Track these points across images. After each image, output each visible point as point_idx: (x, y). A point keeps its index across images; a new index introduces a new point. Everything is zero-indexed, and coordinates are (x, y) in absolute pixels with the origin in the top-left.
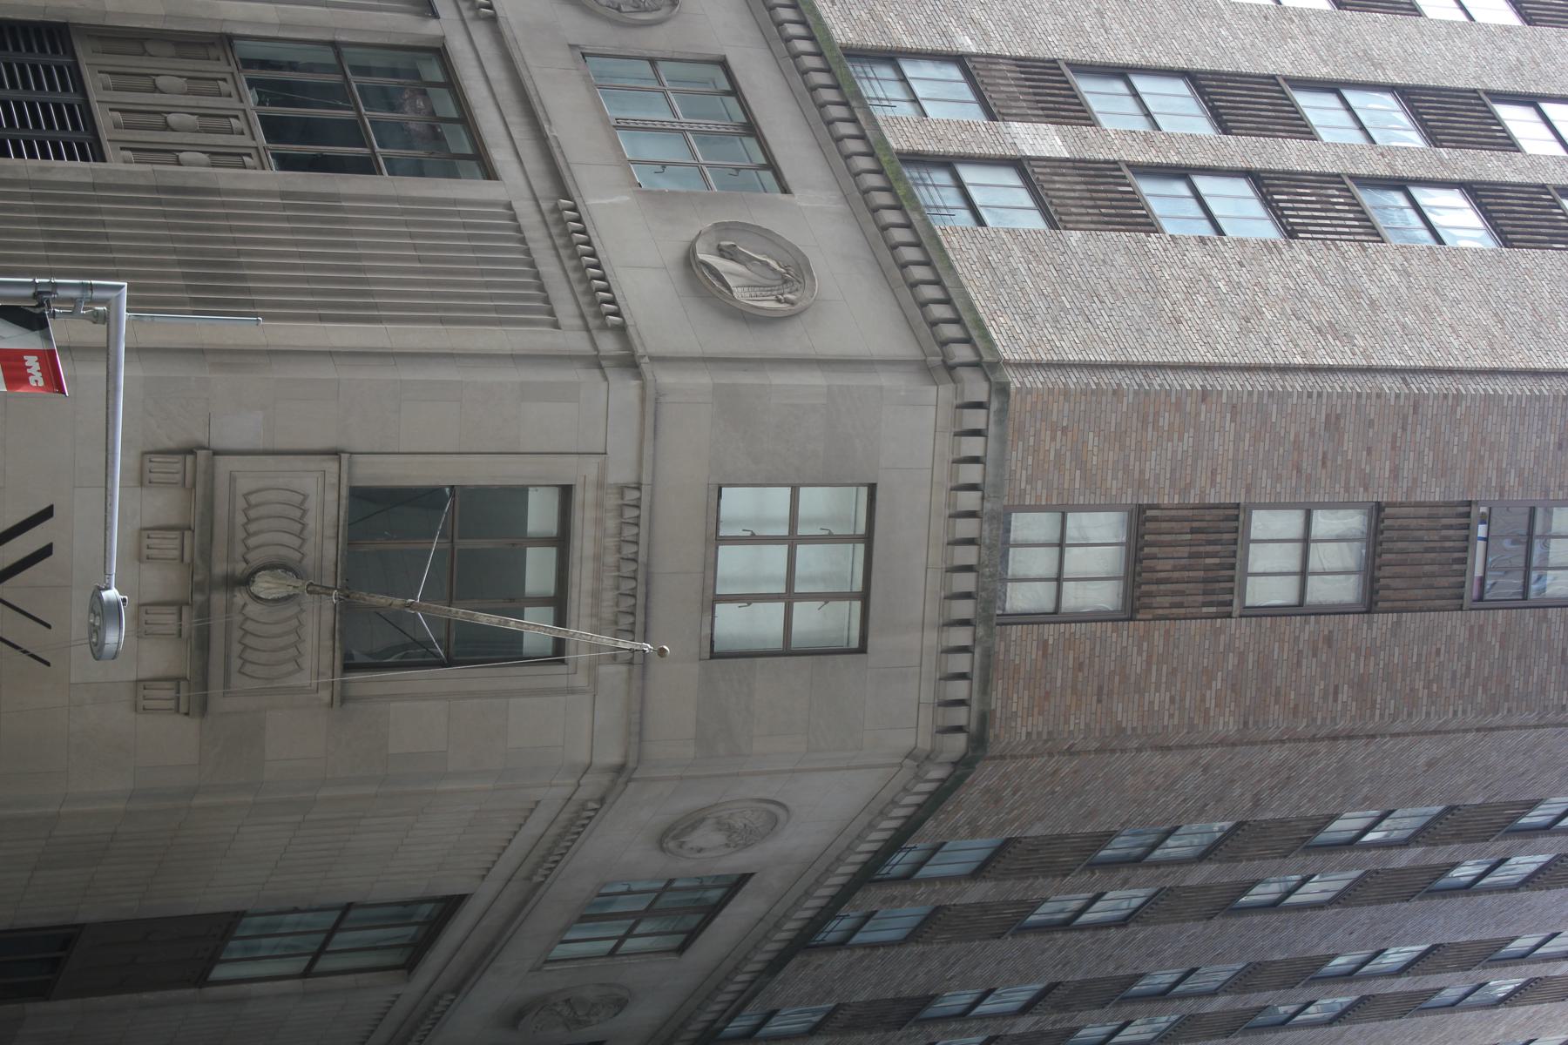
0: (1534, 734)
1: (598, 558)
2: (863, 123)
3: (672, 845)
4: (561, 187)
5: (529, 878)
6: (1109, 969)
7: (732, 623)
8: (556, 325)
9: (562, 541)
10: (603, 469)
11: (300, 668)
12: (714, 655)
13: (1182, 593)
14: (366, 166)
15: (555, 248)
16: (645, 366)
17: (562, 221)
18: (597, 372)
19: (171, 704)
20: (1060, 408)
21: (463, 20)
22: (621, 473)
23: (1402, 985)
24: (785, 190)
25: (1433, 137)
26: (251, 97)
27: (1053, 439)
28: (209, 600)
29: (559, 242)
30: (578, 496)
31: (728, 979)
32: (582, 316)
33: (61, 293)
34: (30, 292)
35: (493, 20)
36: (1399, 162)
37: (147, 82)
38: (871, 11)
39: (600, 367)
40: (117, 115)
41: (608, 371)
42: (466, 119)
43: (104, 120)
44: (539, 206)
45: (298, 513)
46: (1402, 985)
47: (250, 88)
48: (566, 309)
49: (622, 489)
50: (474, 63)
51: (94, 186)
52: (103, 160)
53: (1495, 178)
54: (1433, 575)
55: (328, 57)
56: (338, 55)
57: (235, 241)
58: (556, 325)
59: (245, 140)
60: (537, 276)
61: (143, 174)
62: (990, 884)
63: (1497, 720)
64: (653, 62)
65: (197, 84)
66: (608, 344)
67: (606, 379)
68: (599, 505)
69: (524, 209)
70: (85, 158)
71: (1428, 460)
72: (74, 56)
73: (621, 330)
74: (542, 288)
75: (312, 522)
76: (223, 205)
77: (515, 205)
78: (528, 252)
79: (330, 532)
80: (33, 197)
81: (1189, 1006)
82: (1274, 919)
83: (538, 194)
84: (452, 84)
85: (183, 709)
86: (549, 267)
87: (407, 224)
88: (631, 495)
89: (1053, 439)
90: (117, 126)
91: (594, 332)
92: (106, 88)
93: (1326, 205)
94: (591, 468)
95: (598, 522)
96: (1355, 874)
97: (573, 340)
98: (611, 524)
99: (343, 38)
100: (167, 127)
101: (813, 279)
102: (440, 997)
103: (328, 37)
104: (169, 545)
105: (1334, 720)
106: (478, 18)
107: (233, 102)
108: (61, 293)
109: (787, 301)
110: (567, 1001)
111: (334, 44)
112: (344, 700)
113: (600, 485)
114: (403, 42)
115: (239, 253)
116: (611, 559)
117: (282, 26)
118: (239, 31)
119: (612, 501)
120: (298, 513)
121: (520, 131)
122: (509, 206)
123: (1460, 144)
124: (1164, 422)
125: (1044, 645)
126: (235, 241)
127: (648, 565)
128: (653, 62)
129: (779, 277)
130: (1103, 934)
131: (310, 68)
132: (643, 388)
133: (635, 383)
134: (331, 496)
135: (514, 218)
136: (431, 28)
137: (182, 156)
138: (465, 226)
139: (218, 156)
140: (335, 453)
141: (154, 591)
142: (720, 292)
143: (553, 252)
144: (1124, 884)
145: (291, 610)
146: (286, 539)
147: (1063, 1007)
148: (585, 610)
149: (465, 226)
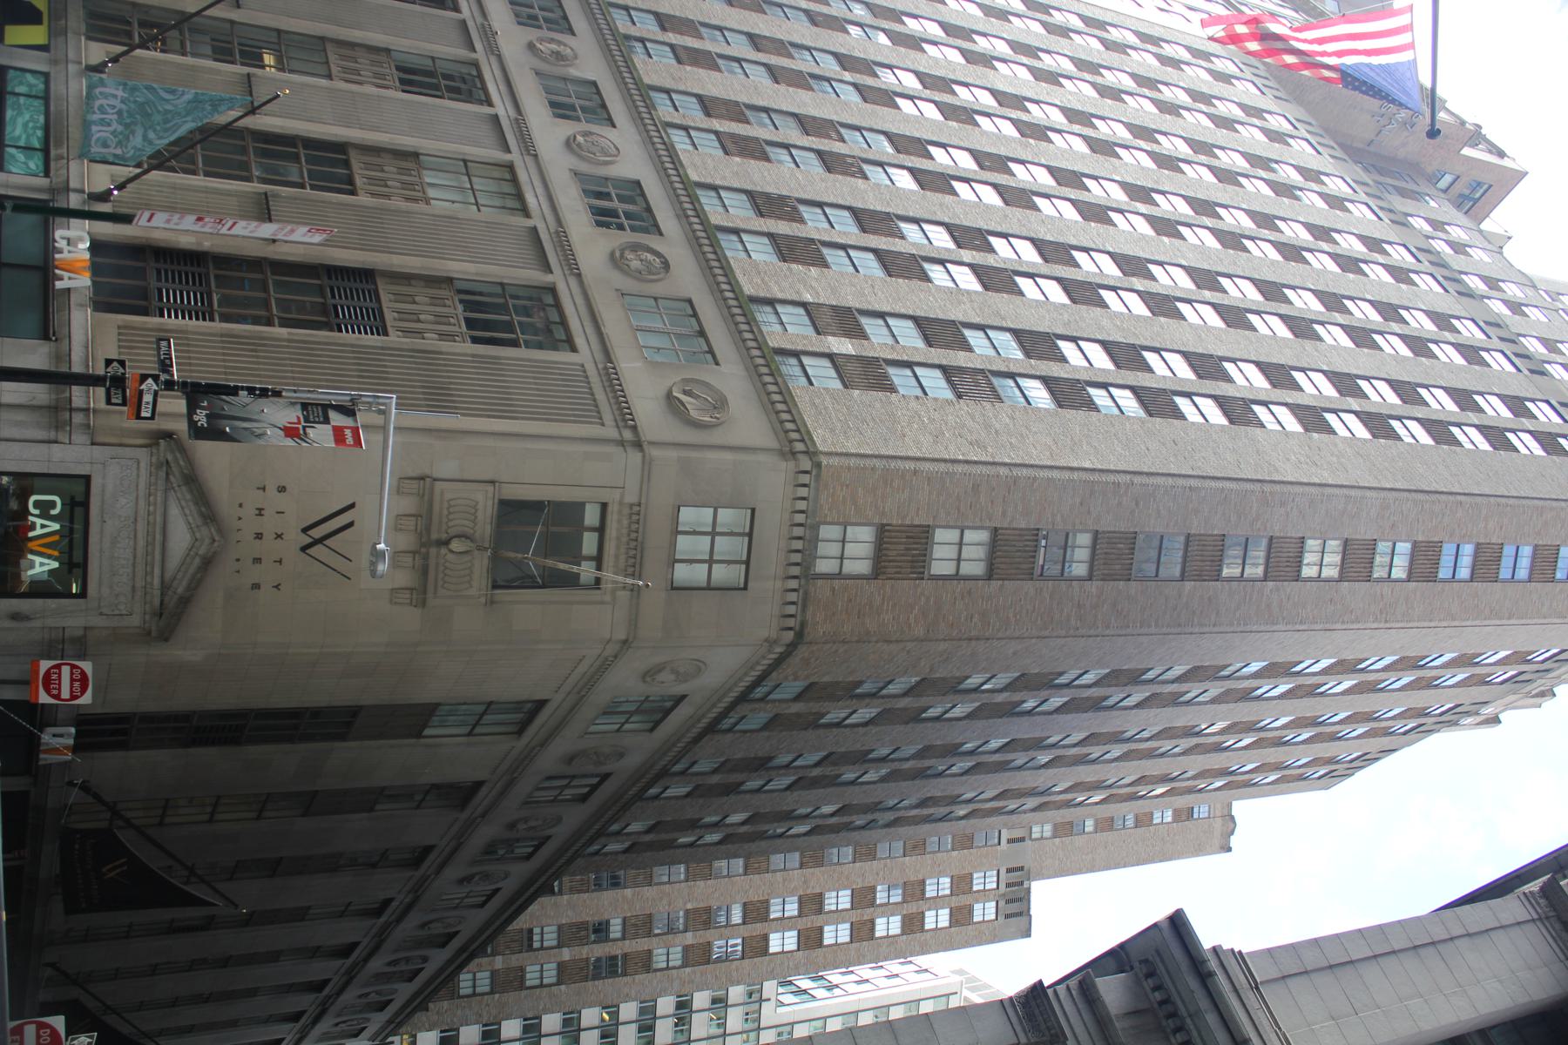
0: (1062, 641)
1: (618, 539)
3: (648, 679)
4: (608, 356)
5: (579, 693)
6: (858, 747)
7: (682, 573)
8: (603, 425)
9: (601, 530)
10: (622, 496)
11: (471, 587)
12: (673, 588)
13: (900, 567)
14: (514, 343)
15: (604, 387)
16: (645, 446)
17: (608, 374)
18: (621, 448)
19: (408, 601)
21: (565, 275)
22: (631, 498)
23: (997, 757)
24: (717, 364)
25: (1028, 354)
26: (460, 308)
27: (842, 490)
28: (428, 553)
29: (606, 384)
30: (610, 509)
31: (674, 745)
32: (616, 421)
33: (364, 399)
34: (348, 398)
35: (579, 276)
36: (1012, 365)
37: (410, 299)
38: (763, 280)
39: (623, 446)
40: (395, 314)
42: (564, 323)
43: (389, 316)
44: (597, 366)
45: (473, 511)
46: (997, 757)
48: (608, 417)
49: (631, 506)
50: (569, 296)
51: (382, 348)
52: (387, 335)
53: (1056, 375)
54: (1020, 563)
55: (499, 290)
56: (504, 289)
57: (449, 377)
58: (603, 425)
59: (456, 329)
60: (595, 400)
61: (406, 343)
62: (802, 704)
63: (1046, 633)
64: (656, 299)
65: (434, 301)
66: (628, 435)
68: (620, 512)
70: (378, 334)
71: (1020, 508)
73: (634, 428)
74: (597, 406)
75: (480, 514)
76: (444, 359)
78: (590, 388)
79: (489, 520)
80: (353, 352)
81: (896, 765)
82: (938, 725)
84: (558, 305)
85: (414, 603)
86: (600, 396)
87: (533, 372)
88: (636, 509)
89: (842, 490)
90: (395, 319)
91: (622, 429)
92: (391, 301)
93: (977, 384)
94: (616, 495)
95: (619, 521)
96: (977, 704)
97: (611, 432)
98: (625, 522)
99: (505, 281)
100: (419, 321)
102: (534, 748)
103: (499, 281)
104: (411, 523)
105: (970, 632)
107: (451, 310)
108: (364, 399)
109: (716, 418)
110: (595, 753)
111: (502, 284)
112: (492, 602)
113: (621, 503)
114: (535, 284)
115: (451, 383)
116: (624, 539)
117: (477, 274)
118: (456, 276)
119: (626, 511)
120: (473, 511)
121: (590, 330)
122: (583, 366)
123: (1040, 358)
124: (895, 484)
125: (833, 590)
126: (449, 377)
127: (642, 543)
128: (656, 299)
130: (856, 730)
131: (490, 295)
132: (644, 456)
133: (640, 454)
134: (490, 503)
135: (585, 371)
136: (549, 278)
137: (425, 335)
138: (560, 374)
139: (443, 336)
140: (492, 482)
141: (402, 547)
144: (866, 707)
145: (467, 558)
146: (466, 523)
147: (835, 764)
148: (611, 564)
149: (560, 374)
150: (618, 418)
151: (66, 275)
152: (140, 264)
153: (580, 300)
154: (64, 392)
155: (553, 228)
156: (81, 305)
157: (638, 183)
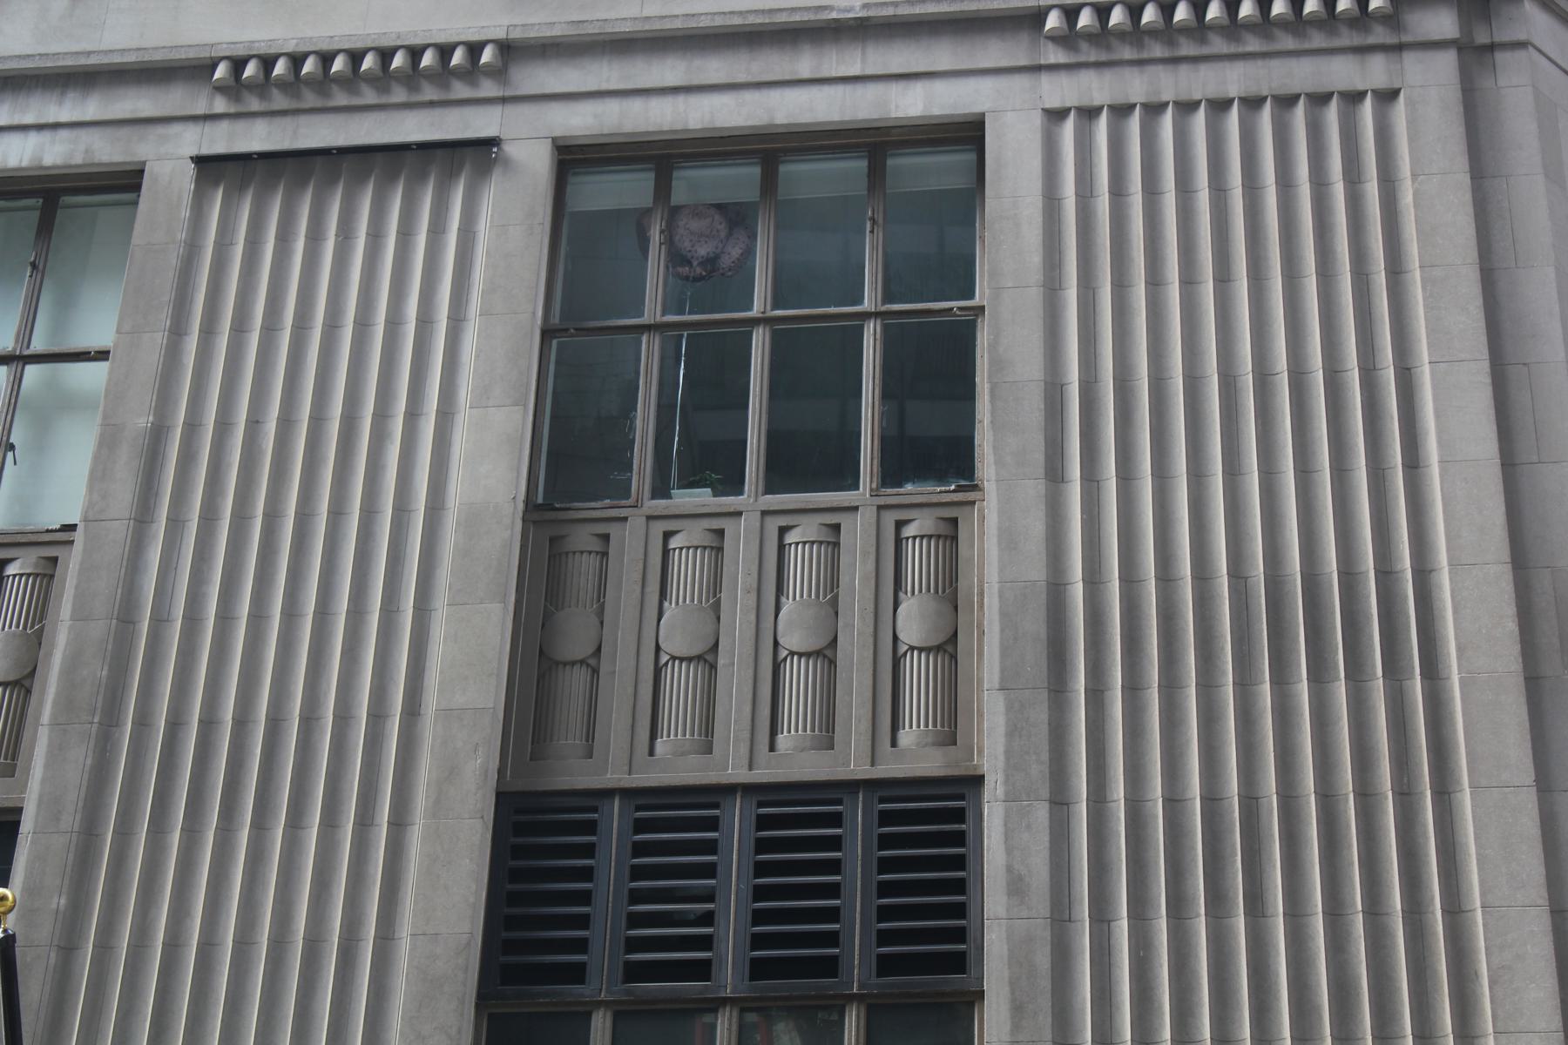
15: (1175, 61)
18: (1501, 57)
21: (504, 100)
35: (509, 50)
39: (1492, 48)
41: (1502, 36)
47: (669, 497)
50: (681, 101)
51: (1060, 802)
67: (1521, 45)
72: (608, 793)
77: (1054, 103)
83: (1023, 61)
87: (1121, 286)
91: (1406, 38)
106: (499, 73)
143: (1184, 69)
150: (1356, 39)
153: (714, 68)
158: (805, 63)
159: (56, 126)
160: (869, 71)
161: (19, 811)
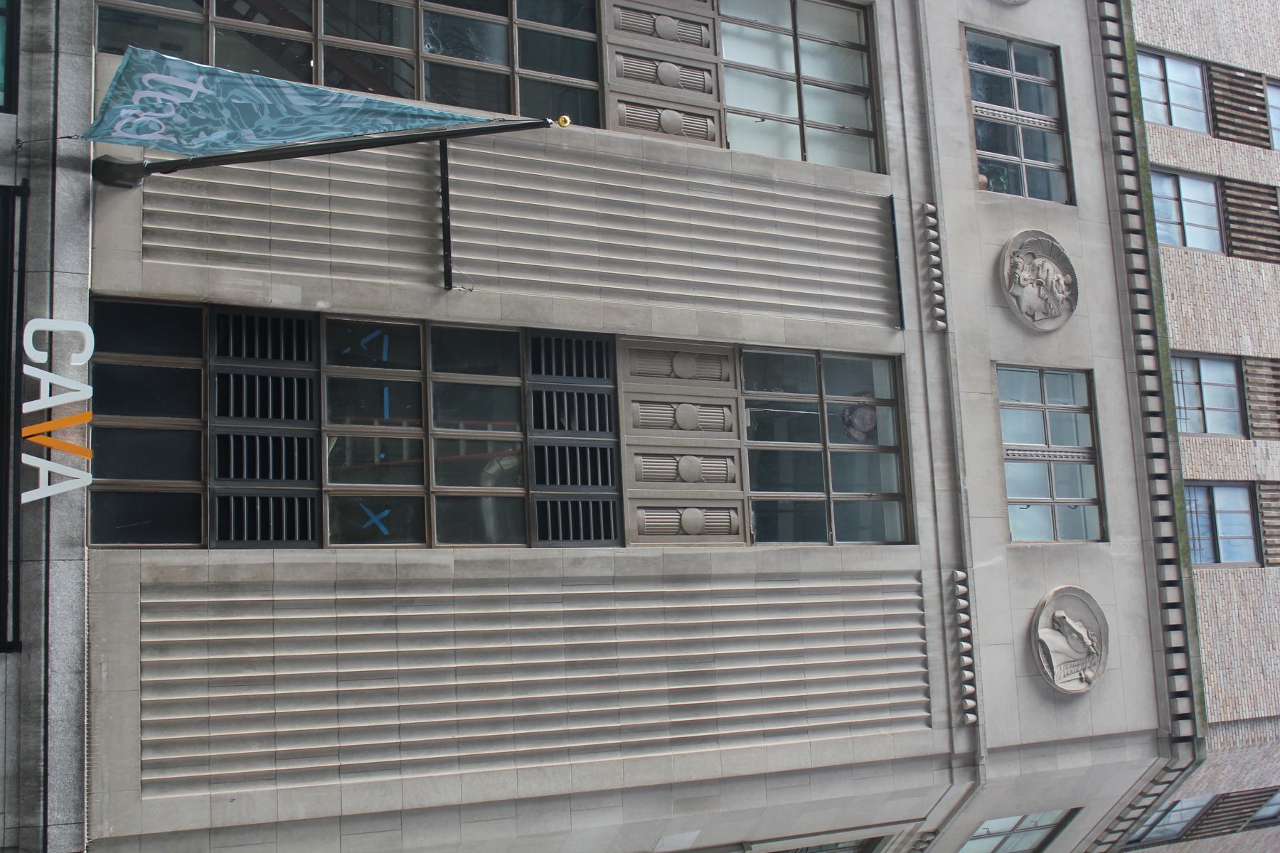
2: (1172, 461)
8: (930, 725)
15: (943, 629)
18: (946, 772)
20: (1219, 740)
21: (921, 331)
35: (944, 333)
39: (950, 768)
41: (955, 771)
47: (746, 407)
50: (923, 410)
67: (952, 781)
69: (930, 578)
72: (615, 383)
77: (924, 576)
84: (897, 402)
87: (843, 606)
101: (1107, 653)
106: (933, 329)
129: (1086, 650)
136: (894, 344)
142: (1046, 673)
143: (940, 633)
151: (43, 466)
152: (189, 363)
153: (938, 424)
154: (32, 810)
155: (917, 199)
156: (71, 544)
157: (1055, 51)
158: (940, 464)
159: (905, 136)
160: (937, 493)
161: (605, 128)
